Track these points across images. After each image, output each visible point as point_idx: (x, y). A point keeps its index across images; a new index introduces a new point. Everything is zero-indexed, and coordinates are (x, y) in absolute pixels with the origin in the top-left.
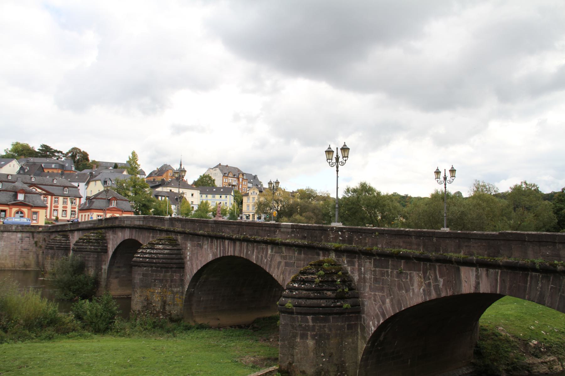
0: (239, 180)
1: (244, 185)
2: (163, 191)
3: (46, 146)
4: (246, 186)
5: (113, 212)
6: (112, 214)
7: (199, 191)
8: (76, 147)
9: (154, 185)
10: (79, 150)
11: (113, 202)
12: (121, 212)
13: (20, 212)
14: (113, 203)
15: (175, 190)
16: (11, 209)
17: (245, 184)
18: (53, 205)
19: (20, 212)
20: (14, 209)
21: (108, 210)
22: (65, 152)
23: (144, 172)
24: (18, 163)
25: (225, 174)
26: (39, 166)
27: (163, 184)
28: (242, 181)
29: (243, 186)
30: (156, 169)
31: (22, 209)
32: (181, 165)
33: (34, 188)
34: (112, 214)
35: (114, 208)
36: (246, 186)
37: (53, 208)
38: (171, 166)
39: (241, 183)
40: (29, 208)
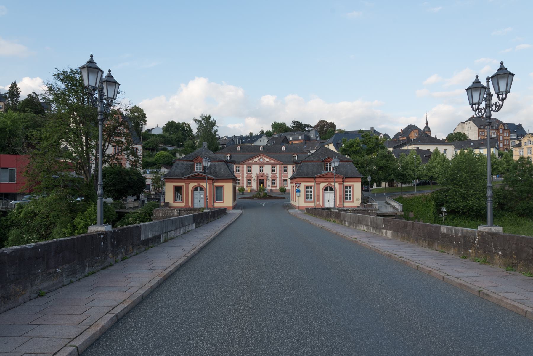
0: (499, 132)
1: (506, 136)
2: (408, 150)
3: (298, 122)
4: (508, 138)
5: (329, 180)
6: (327, 183)
7: (453, 147)
8: (322, 119)
9: (398, 144)
10: (326, 122)
11: (328, 165)
12: (341, 180)
13: (199, 188)
14: (328, 167)
15: (423, 147)
16: (187, 184)
17: (508, 135)
18: (283, 174)
19: (199, 188)
20: (192, 185)
21: (320, 177)
22: (313, 126)
23: (389, 136)
24: (267, 138)
25: (481, 126)
26: (283, 138)
27: (409, 142)
28: (503, 132)
29: (505, 138)
30: (400, 131)
31: (202, 184)
32: (427, 123)
33: (261, 158)
34: (327, 183)
35: (329, 173)
36: (508, 138)
37: (283, 178)
38: (416, 125)
39: (502, 135)
40: (211, 181)
